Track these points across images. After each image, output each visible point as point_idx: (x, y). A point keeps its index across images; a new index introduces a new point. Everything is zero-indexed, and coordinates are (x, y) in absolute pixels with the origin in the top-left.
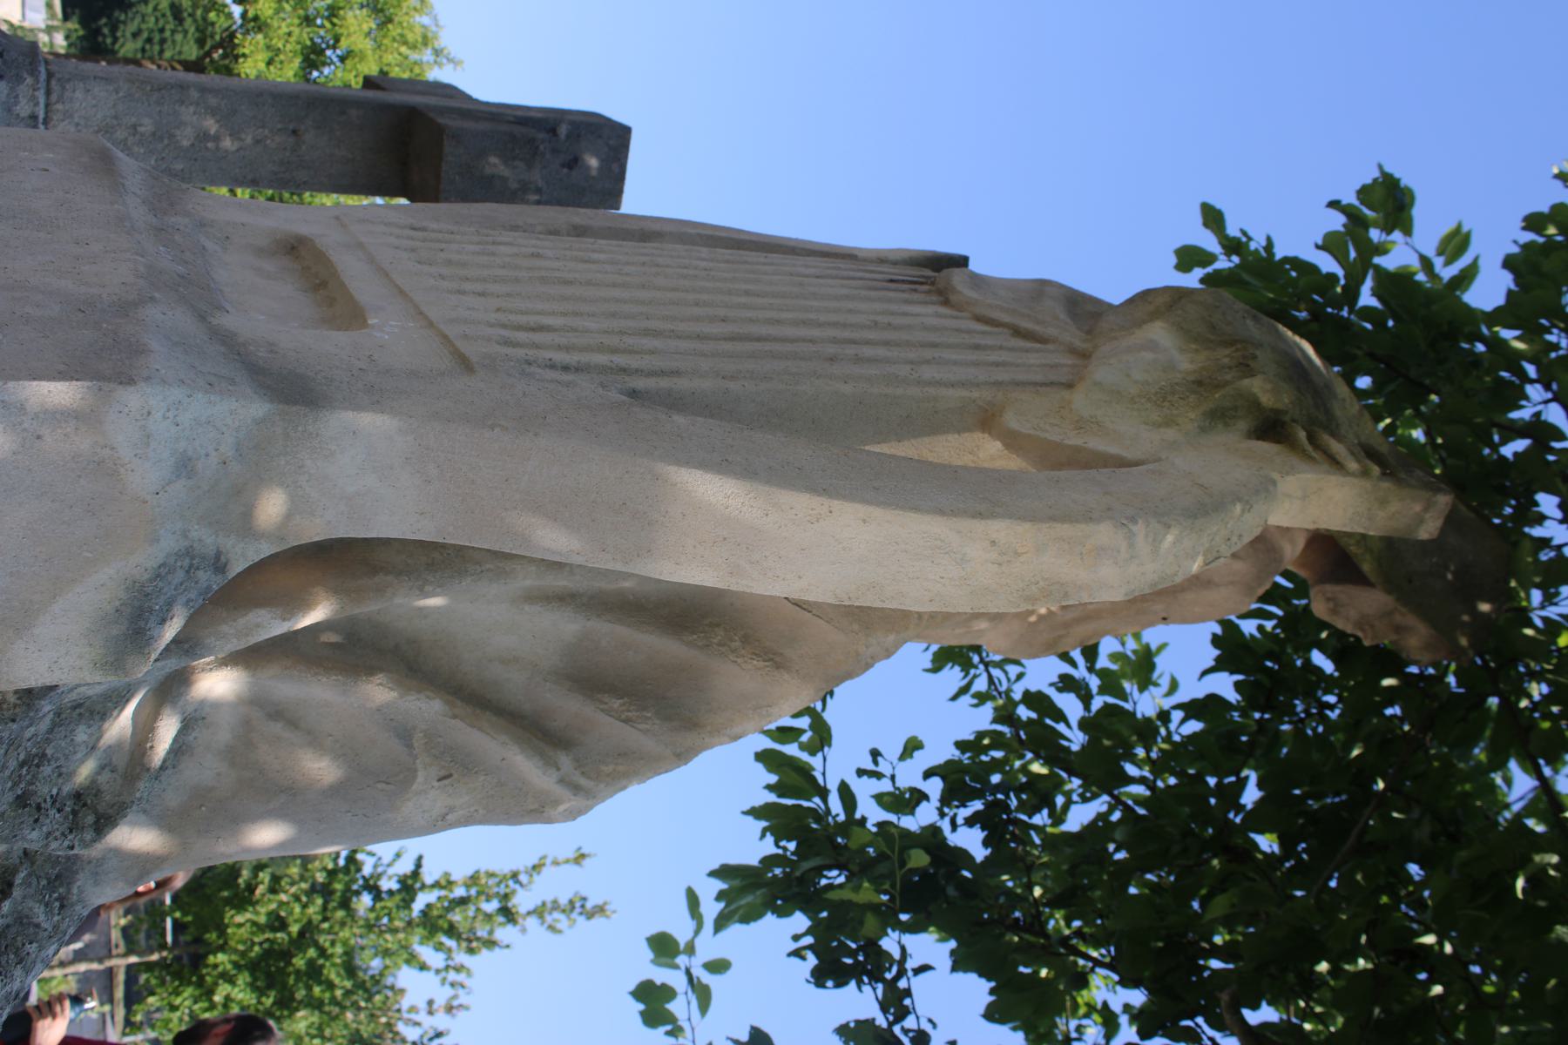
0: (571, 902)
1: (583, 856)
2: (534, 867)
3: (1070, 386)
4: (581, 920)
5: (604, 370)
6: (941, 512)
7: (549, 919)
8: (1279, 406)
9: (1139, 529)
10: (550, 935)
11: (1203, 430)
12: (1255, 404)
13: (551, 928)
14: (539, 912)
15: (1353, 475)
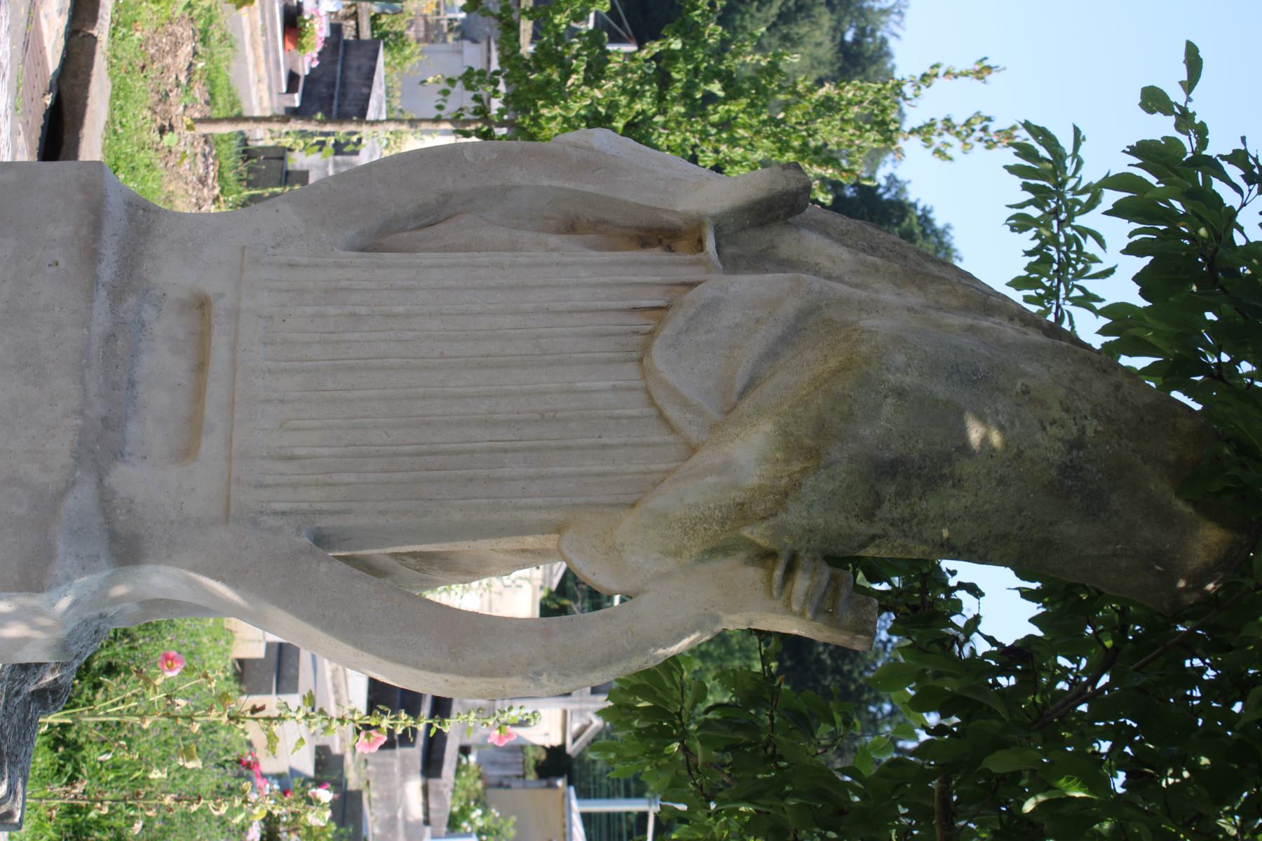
0: (968, 123)
1: (989, 69)
2: (925, 77)
3: (633, 505)
4: (980, 146)
5: (304, 513)
6: (416, 666)
7: (937, 141)
8: (775, 547)
9: (544, 679)
10: (936, 161)
11: (701, 561)
12: (752, 544)
13: (939, 152)
14: (925, 132)
15: (794, 614)
